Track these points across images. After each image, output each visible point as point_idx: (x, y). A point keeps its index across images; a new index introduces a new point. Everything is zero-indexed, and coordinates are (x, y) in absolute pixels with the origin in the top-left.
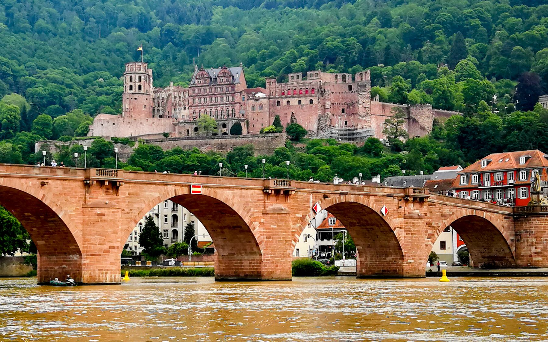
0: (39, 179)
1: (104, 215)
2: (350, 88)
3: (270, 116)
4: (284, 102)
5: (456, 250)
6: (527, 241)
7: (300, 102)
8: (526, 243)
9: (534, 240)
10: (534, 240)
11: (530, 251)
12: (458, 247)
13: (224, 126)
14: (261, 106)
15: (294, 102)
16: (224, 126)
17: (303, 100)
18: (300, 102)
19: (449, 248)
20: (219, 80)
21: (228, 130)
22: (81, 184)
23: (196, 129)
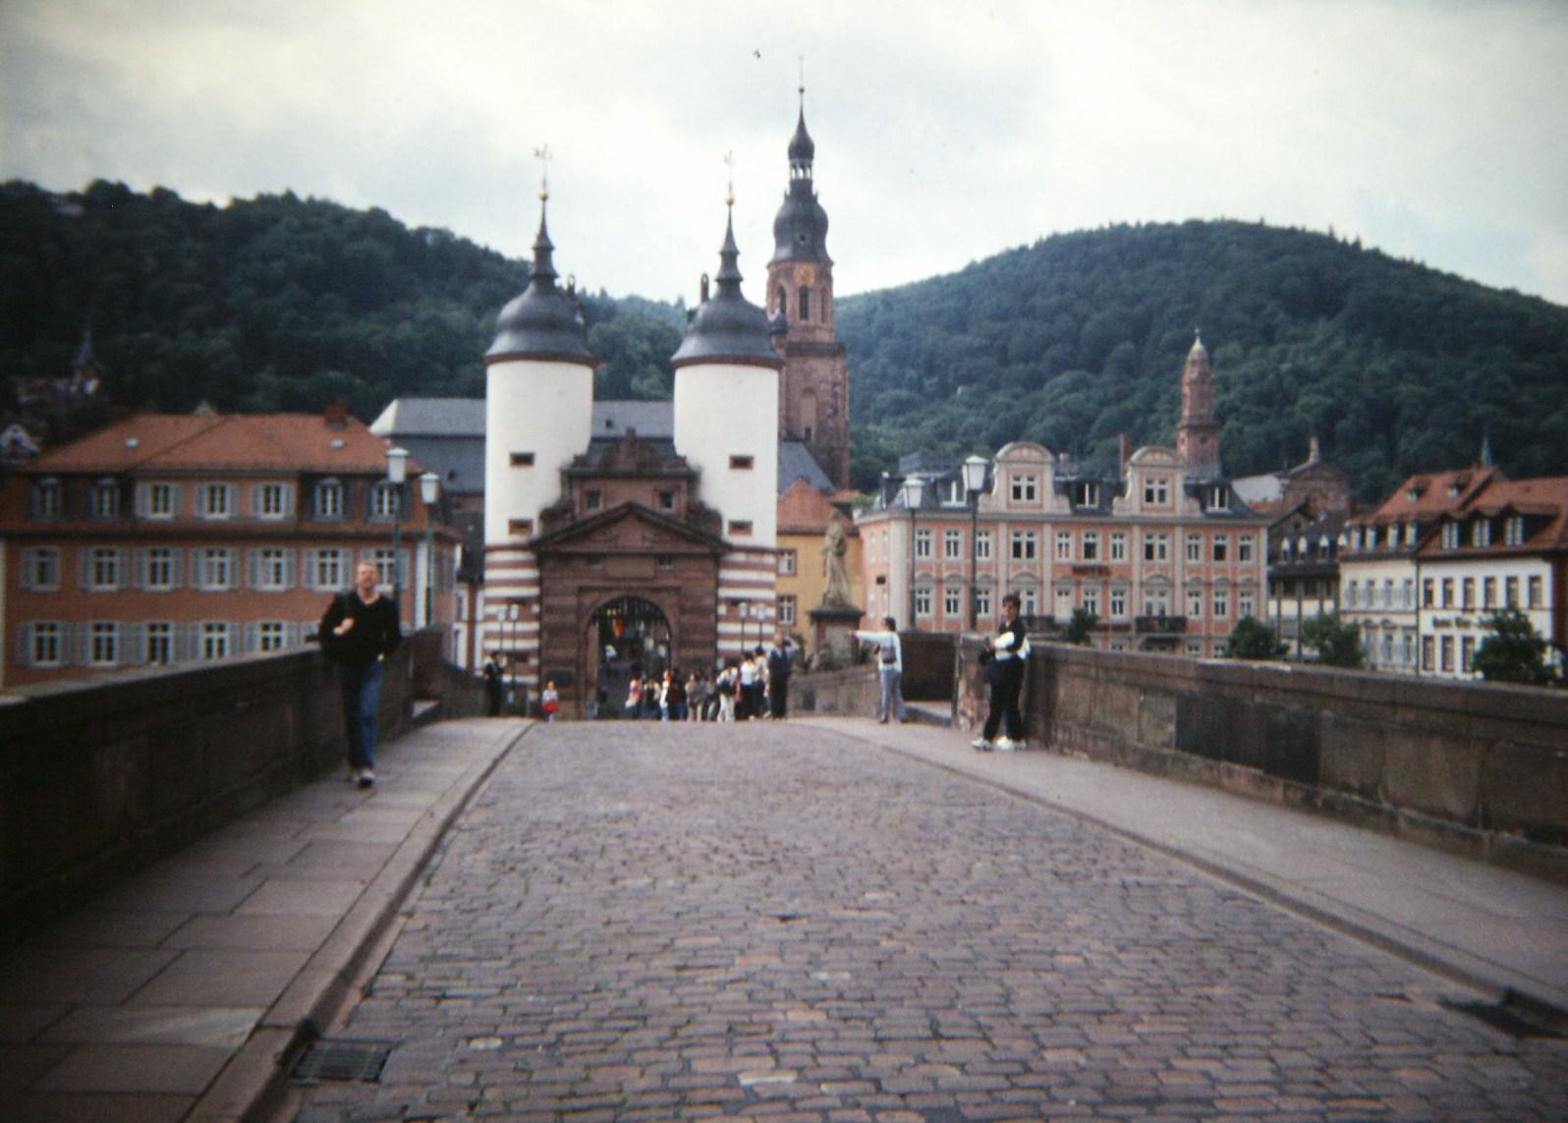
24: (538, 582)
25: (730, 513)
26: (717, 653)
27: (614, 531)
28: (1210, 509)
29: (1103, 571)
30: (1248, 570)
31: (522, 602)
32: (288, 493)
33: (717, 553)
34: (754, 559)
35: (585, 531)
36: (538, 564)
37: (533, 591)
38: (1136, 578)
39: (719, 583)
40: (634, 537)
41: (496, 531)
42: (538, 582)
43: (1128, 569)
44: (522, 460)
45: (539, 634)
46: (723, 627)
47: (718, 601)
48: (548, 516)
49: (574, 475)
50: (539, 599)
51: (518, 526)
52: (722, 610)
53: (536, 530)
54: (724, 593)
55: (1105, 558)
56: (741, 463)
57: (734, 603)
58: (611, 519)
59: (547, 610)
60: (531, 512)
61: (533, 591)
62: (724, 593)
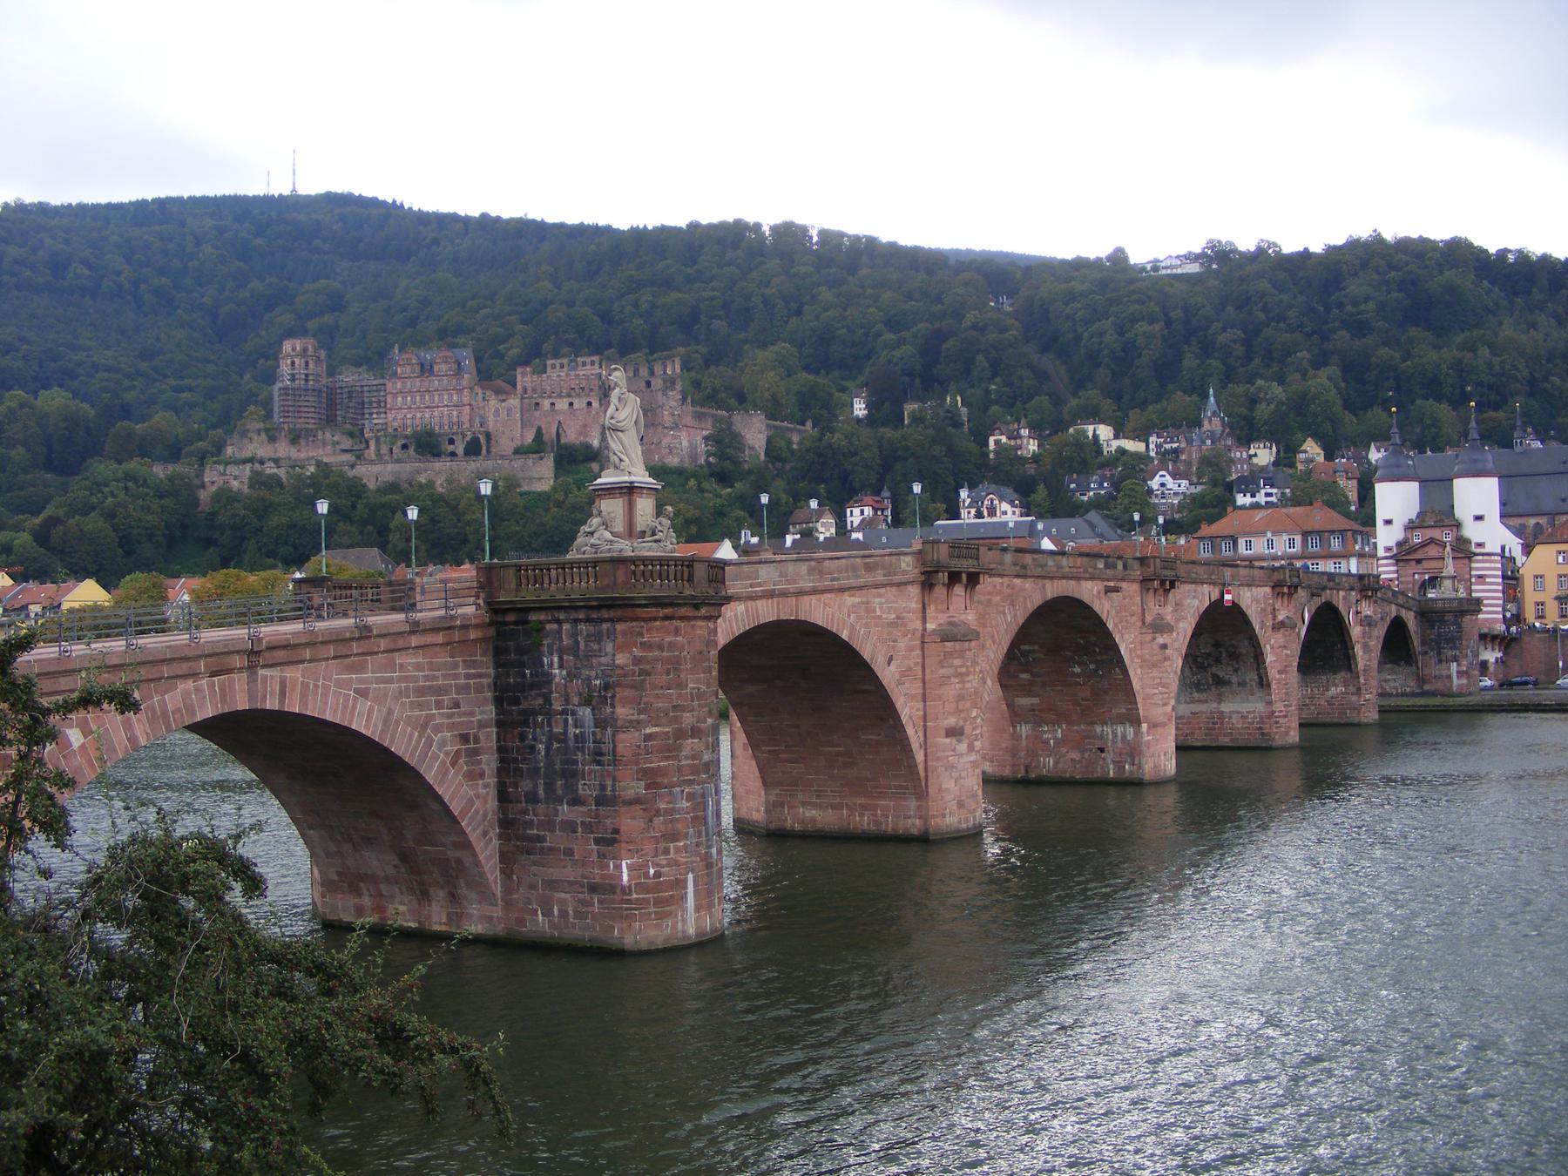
0: (1103, 579)
1: (1164, 646)
2: (648, 384)
3: (524, 424)
4: (546, 404)
7: (571, 404)
13: (451, 442)
14: (509, 410)
15: (562, 405)
16: (451, 442)
17: (575, 401)
18: (571, 404)
20: (436, 368)
21: (460, 450)
22: (1135, 587)
23: (405, 447)
25: (1475, 539)
32: (1298, 539)
33: (1470, 556)
35: (1414, 549)
41: (1381, 553)
44: (1388, 522)
48: (1399, 544)
49: (1410, 527)
51: (1388, 549)
56: (1479, 518)
57: (1480, 577)
58: (1424, 545)
60: (1392, 543)
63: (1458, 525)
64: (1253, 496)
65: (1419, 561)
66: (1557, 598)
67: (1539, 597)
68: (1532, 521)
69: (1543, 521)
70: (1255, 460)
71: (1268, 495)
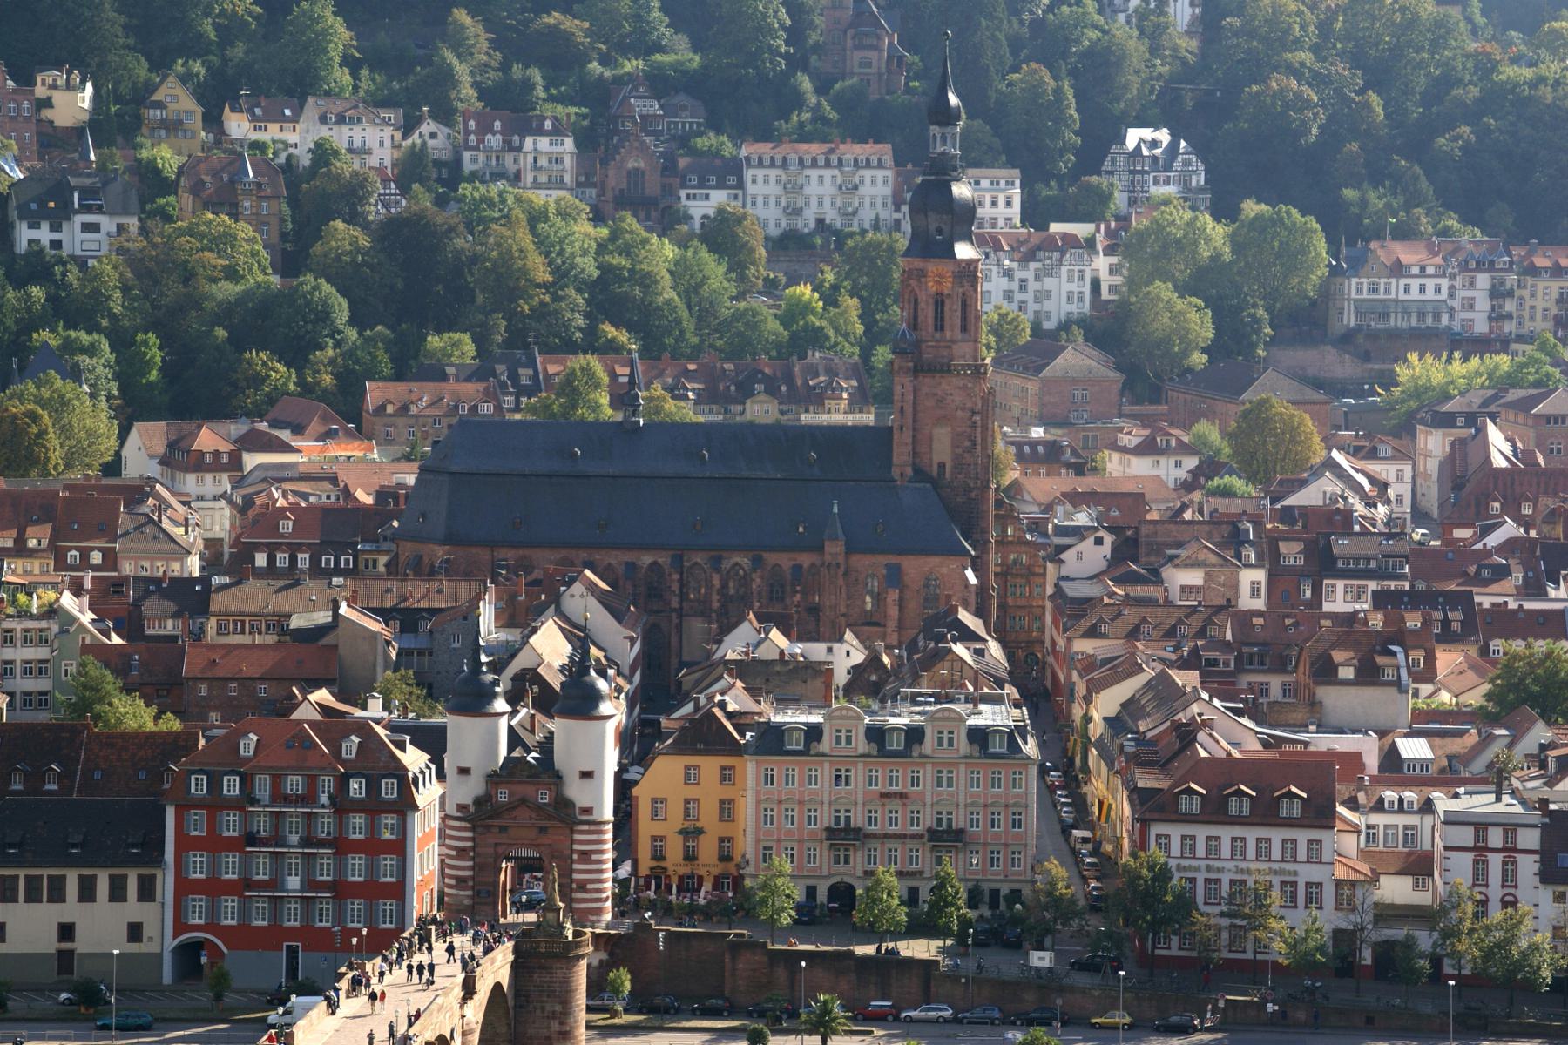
5: (170, 943)
6: (543, 1009)
8: (538, 1012)
9: (558, 1008)
10: (558, 1008)
11: (549, 1028)
12: (175, 938)
19: (151, 939)
24: (473, 839)
26: (572, 881)
27: (515, 813)
28: (991, 750)
29: (902, 796)
30: (1018, 795)
31: (464, 849)
34: (593, 828)
35: (498, 811)
36: (473, 829)
37: (469, 844)
38: (928, 801)
39: (573, 842)
40: (523, 815)
42: (473, 839)
43: (923, 793)
44: (464, 771)
45: (472, 868)
46: (576, 866)
47: (572, 851)
48: (478, 802)
49: (493, 778)
50: (473, 849)
51: (461, 807)
52: (575, 856)
53: (472, 809)
54: (576, 847)
55: (904, 786)
56: (587, 775)
58: (511, 807)
59: (477, 855)
60: (468, 800)
61: (469, 844)
62: (576, 847)
63: (558, 777)
64: (55, 228)
65: (503, 829)
66: (681, 832)
67: (658, 829)
68: (646, 559)
69: (664, 559)
70: (47, 114)
71: (87, 228)
